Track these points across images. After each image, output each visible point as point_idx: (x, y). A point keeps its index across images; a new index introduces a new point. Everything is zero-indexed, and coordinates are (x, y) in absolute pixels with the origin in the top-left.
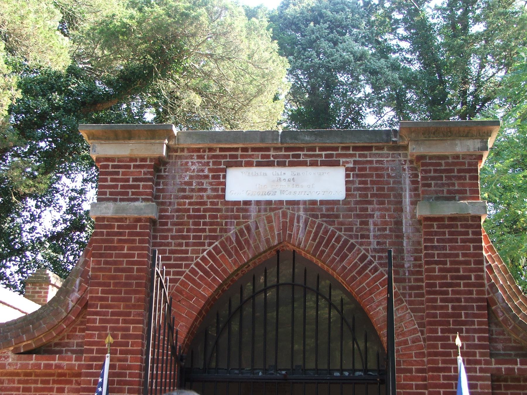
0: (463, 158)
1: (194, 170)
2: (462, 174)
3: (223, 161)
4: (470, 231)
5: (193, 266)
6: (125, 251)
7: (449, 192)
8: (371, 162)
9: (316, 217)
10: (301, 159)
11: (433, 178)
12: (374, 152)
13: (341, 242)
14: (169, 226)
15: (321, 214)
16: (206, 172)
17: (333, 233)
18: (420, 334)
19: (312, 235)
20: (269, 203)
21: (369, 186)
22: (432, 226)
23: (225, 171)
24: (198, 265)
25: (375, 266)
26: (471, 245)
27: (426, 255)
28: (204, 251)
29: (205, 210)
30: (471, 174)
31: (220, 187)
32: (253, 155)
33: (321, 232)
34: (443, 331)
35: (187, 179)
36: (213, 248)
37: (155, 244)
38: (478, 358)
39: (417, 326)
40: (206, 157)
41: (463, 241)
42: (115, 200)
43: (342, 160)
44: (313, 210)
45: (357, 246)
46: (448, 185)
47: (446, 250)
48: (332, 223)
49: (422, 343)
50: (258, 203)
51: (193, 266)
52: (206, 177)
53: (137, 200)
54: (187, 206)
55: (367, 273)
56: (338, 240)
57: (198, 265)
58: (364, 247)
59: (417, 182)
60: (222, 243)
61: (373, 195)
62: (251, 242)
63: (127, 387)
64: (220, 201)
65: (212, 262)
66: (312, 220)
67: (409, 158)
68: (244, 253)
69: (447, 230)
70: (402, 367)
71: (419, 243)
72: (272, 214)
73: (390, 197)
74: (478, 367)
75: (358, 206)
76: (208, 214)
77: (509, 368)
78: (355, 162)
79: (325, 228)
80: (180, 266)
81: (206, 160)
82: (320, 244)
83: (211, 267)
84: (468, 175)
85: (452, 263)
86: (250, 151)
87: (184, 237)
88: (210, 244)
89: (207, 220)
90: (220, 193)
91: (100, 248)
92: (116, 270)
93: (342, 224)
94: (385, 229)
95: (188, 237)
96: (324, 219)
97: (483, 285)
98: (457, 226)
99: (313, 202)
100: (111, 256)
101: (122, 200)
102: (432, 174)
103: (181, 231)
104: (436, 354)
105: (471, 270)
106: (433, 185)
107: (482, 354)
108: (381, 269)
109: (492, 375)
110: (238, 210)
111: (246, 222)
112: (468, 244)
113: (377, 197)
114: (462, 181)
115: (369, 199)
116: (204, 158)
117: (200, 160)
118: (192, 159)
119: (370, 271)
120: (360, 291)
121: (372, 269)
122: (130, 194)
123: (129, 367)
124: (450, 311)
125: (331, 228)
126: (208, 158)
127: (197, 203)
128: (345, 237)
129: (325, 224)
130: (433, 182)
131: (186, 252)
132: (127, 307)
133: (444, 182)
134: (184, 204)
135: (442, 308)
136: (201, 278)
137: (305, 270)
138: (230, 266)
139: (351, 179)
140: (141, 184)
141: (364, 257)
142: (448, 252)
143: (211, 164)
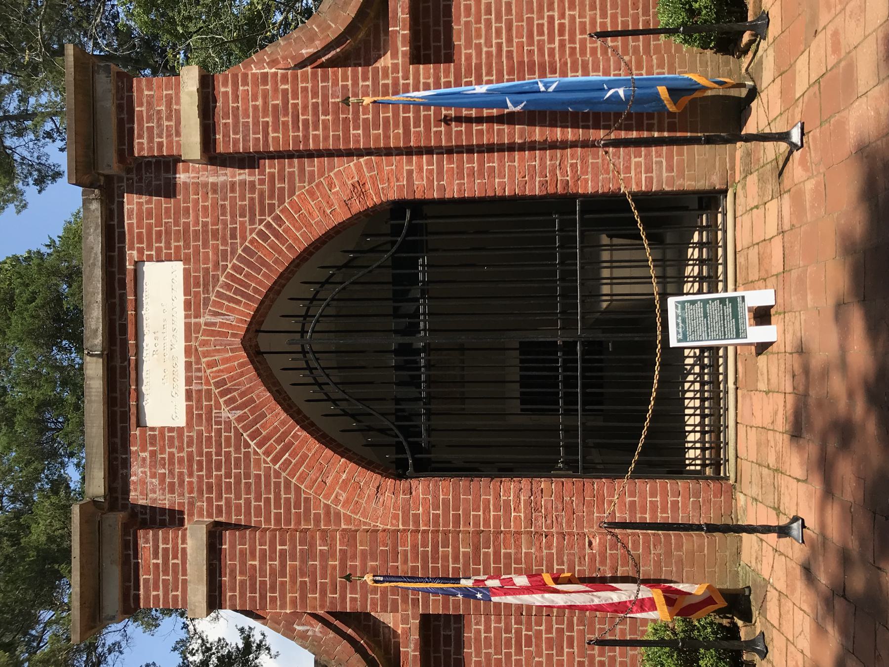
0: (122, 98)
1: (142, 472)
2: (145, 100)
5: (277, 467)
6: (257, 563)
7: (169, 118)
9: (207, 301)
16: (146, 454)
17: (230, 277)
19: (231, 305)
20: (188, 366)
21: (163, 228)
24: (275, 461)
25: (273, 219)
26: (241, 88)
28: (256, 453)
31: (167, 434)
32: (120, 390)
33: (228, 293)
35: (156, 481)
38: (390, 81)
41: (236, 98)
42: (185, 582)
46: (159, 119)
48: (216, 279)
50: (189, 381)
52: (153, 454)
53: (184, 550)
54: (195, 480)
56: (238, 270)
58: (248, 233)
61: (177, 224)
62: (243, 389)
63: (441, 549)
64: (186, 434)
65: (272, 441)
67: (124, 174)
70: (405, 183)
74: (401, 82)
75: (192, 244)
76: (205, 450)
79: (222, 287)
80: (277, 485)
82: (244, 294)
83: (278, 441)
85: (265, 115)
86: (114, 395)
87: (238, 482)
88: (247, 445)
89: (214, 450)
93: (216, 265)
94: (223, 207)
99: (187, 305)
100: (263, 583)
101: (185, 573)
105: (276, 89)
106: (160, 140)
109: (412, 63)
111: (216, 396)
112: (240, 93)
113: (179, 217)
115: (181, 228)
119: (280, 226)
121: (277, 225)
122: (175, 561)
123: (415, 547)
125: (222, 279)
127: (190, 466)
128: (234, 261)
129: (217, 289)
130: (156, 140)
133: (154, 125)
135: (326, 128)
136: (293, 455)
137: (283, 316)
139: (153, 253)
140: (161, 546)
141: (261, 234)
142: (250, 120)
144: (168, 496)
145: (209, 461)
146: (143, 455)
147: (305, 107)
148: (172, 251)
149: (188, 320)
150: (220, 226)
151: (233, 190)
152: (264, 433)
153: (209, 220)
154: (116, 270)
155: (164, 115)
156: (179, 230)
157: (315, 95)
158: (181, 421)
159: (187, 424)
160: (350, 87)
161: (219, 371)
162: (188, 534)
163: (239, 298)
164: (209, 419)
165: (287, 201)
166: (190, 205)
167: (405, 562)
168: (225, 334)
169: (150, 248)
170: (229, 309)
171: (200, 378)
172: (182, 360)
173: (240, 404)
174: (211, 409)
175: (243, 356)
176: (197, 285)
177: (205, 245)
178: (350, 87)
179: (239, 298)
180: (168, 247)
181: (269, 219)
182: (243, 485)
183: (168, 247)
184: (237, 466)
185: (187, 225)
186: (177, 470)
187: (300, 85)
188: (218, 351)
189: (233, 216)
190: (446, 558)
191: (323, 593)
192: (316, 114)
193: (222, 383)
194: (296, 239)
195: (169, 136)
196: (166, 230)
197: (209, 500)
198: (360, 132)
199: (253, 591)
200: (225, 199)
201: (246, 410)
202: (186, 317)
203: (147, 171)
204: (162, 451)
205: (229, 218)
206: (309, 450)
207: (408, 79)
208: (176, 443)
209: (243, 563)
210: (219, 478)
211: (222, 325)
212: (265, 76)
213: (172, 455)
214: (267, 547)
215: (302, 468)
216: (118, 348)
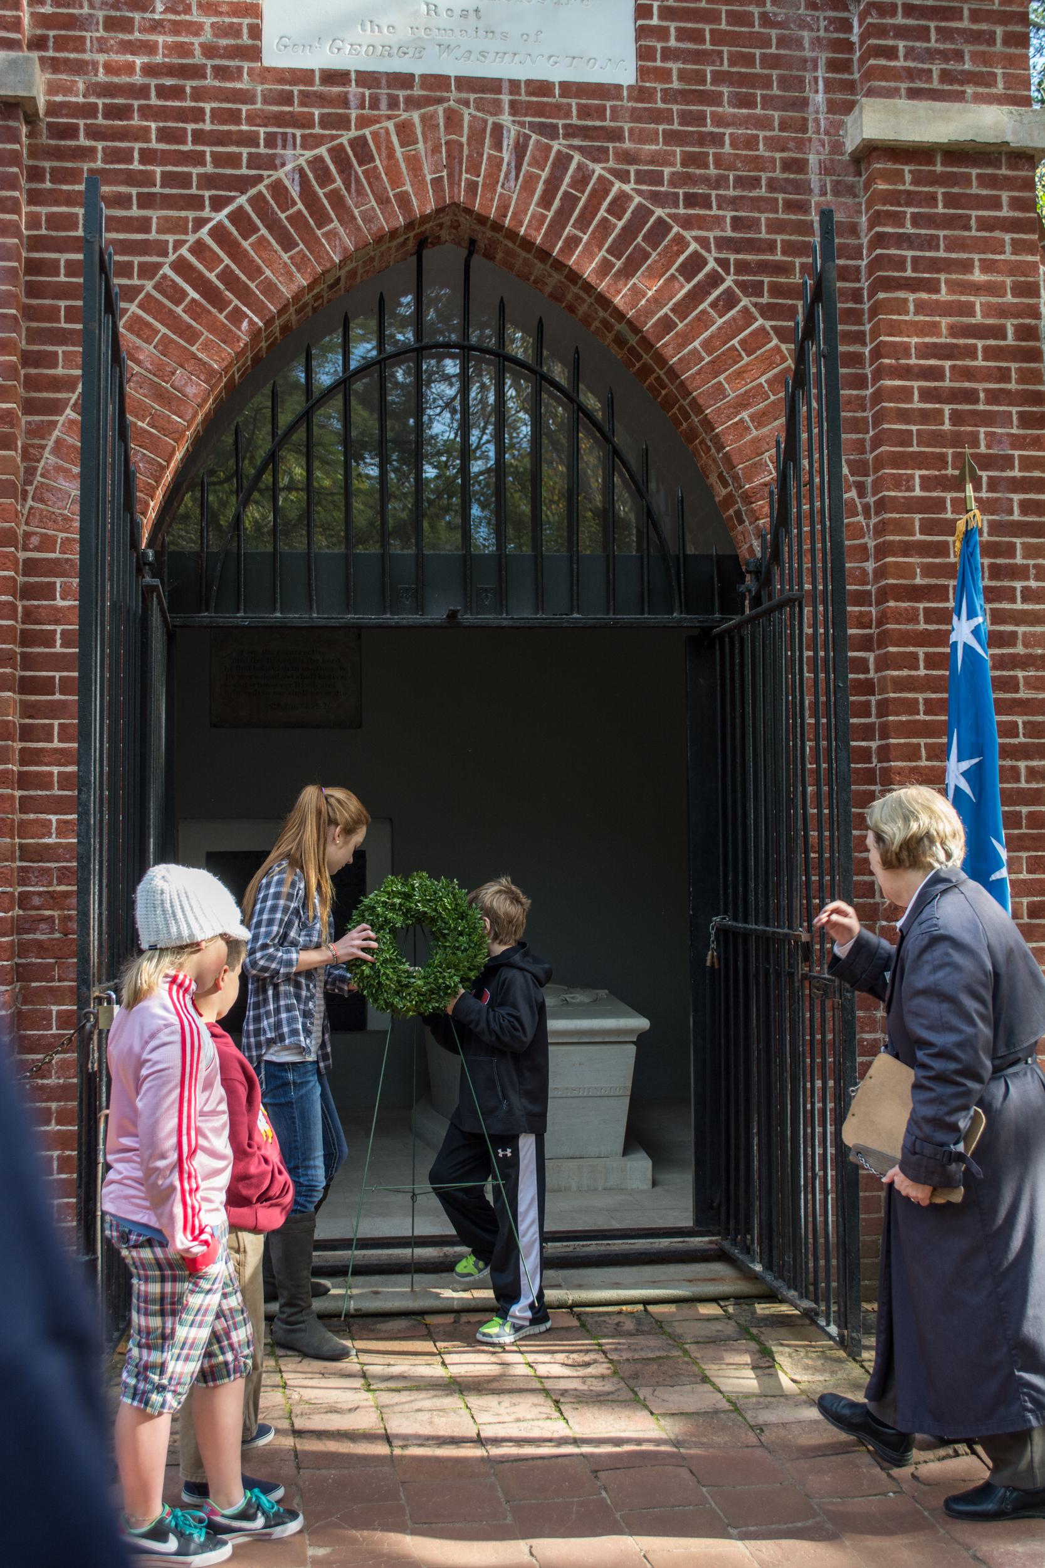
2: (984, 26)
4: (1005, 196)
5: (166, 270)
9: (550, 131)
11: (901, 32)
13: (628, 215)
14: (83, 141)
15: (565, 126)
17: (604, 187)
19: (540, 187)
20: (404, 80)
21: (708, 46)
22: (898, 176)
24: (181, 266)
25: (729, 290)
26: (1007, 237)
27: (876, 264)
28: (200, 223)
30: (1010, 28)
31: (246, 21)
33: (567, 180)
34: (926, 483)
37: (34, 198)
38: (1019, 560)
41: (985, 225)
45: (676, 229)
46: (945, 56)
47: (937, 249)
48: (598, 155)
49: (860, 518)
50: (367, 79)
54: (138, 79)
57: (181, 266)
59: (849, 46)
60: (258, 202)
61: (718, 77)
64: (246, 65)
65: (227, 261)
66: (538, 141)
69: (940, 191)
72: (416, 116)
73: (769, 86)
74: (1018, 585)
75: (675, 107)
76: (208, 107)
79: (580, 167)
83: (227, 277)
84: (999, 31)
87: (131, 178)
88: (218, 204)
89: (208, 126)
90: (245, 40)
93: (628, 157)
94: (755, 183)
95: (146, 179)
96: (577, 142)
98: (966, 180)
99: (542, 88)
102: (900, 20)
103: (125, 156)
104: (907, 549)
105: (1003, 312)
106: (901, 53)
108: (745, 301)
110: (307, 98)
112: (997, 234)
113: (731, 84)
115: (709, 87)
119: (713, 305)
120: (687, 362)
121: (718, 299)
124: (947, 426)
125: (598, 169)
128: (637, 199)
129: (577, 158)
130: (901, 44)
131: (143, 225)
133: (933, 44)
134: (130, 68)
135: (925, 416)
136: (194, 309)
139: (655, 21)
141: (694, 264)
142: (942, 254)
144: (100, 14)
145: (183, 115)
147: (968, 374)
148: (659, 63)
149: (506, 87)
150: (712, 171)
151: (790, 206)
152: (246, 244)
153: (727, 149)
155: (951, 66)
156: (703, 82)
157: (994, 397)
159: (268, 70)
160: (1009, 474)
162: (13, 54)
163: (557, 203)
164: (280, 120)
165: (768, 324)
166: (758, 111)
168: (474, 169)
170: (532, 179)
171: (375, 105)
172: (418, 69)
173: (315, 193)
174: (303, 126)
175: (424, 204)
176: (584, 112)
177: (672, 137)
178: (1009, 474)
179: (557, 203)
180: (667, 54)
181: (729, 282)
182: (123, 189)
183: (667, 54)
185: (714, 99)
186: (161, 39)
187: (1014, 366)
188: (436, 150)
189: (735, 203)
192: (954, 396)
193: (365, 157)
194: (685, 338)
195: (911, 74)
197: (89, 111)
198: (918, 492)
200: (772, 185)
201: (300, 206)
202: (514, 85)
203: (831, 21)
205: (731, 193)
206: (206, 347)
207: (1025, 600)
208: (224, 42)
211: (496, 163)
215: (164, 330)
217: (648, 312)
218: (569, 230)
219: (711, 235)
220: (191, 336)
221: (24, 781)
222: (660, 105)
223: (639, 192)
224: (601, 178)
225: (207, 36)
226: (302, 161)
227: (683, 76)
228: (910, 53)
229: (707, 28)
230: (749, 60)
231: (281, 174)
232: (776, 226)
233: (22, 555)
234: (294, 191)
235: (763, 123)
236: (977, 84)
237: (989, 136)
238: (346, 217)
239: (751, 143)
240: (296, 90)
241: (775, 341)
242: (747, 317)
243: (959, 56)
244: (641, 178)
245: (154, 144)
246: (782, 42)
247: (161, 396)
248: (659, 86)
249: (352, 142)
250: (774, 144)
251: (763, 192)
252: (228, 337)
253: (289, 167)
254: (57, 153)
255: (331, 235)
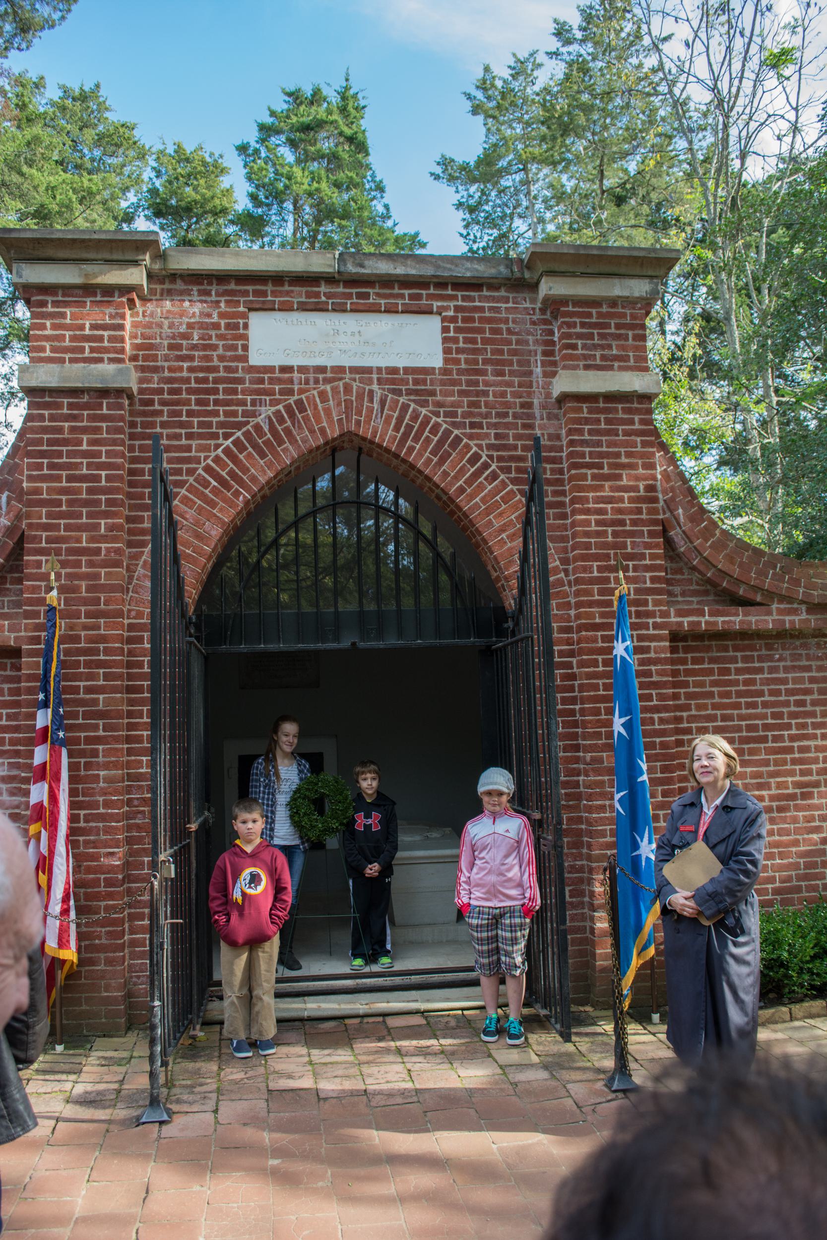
1: (194, 313)
2: (622, 332)
3: (242, 299)
5: (200, 471)
6: (85, 447)
8: (481, 309)
9: (399, 393)
10: (371, 301)
11: (580, 336)
12: (485, 293)
14: (157, 407)
16: (215, 318)
17: (427, 420)
18: (562, 575)
19: (394, 421)
20: (322, 369)
21: (480, 346)
22: (580, 410)
23: (244, 316)
24: (208, 469)
25: (494, 471)
26: (639, 439)
27: (571, 455)
28: (217, 446)
29: (216, 381)
31: (240, 343)
33: (408, 417)
35: (183, 329)
36: (233, 443)
37: (132, 437)
38: (650, 608)
39: (558, 563)
40: (213, 293)
41: (627, 433)
42: (62, 361)
43: (436, 304)
44: (393, 382)
45: (465, 440)
46: (602, 347)
48: (424, 404)
49: (567, 588)
50: (302, 369)
51: (200, 471)
52: (216, 326)
53: (100, 360)
54: (185, 374)
55: (481, 483)
57: (208, 469)
59: (553, 343)
60: (247, 434)
61: (486, 362)
63: (101, 671)
64: (240, 365)
65: (232, 465)
68: (284, 450)
69: (602, 417)
71: (558, 437)
72: (328, 388)
74: (651, 621)
76: (221, 387)
77: (693, 622)
78: (457, 309)
79: (414, 410)
81: (214, 298)
82: (406, 436)
83: (232, 474)
84: (630, 333)
86: (286, 284)
87: (182, 425)
88: (226, 436)
89: (221, 397)
90: (240, 352)
91: (40, 442)
92: (70, 479)
93: (439, 404)
94: (506, 415)
95: (189, 425)
96: (412, 397)
97: (655, 500)
99: (394, 370)
100: (60, 455)
101: (72, 361)
102: (578, 330)
103: (179, 414)
104: (591, 604)
107: (656, 603)
108: (502, 477)
111: (286, 400)
112: (633, 438)
113: (492, 365)
114: (622, 342)
115: (481, 367)
116: (211, 295)
117: (203, 298)
118: (190, 295)
119: (486, 479)
122: (87, 350)
123: (104, 639)
124: (610, 539)
125: (424, 411)
126: (217, 295)
128: (445, 426)
129: (413, 405)
130: (580, 342)
131: (188, 449)
132: (91, 540)
133: (596, 341)
135: (598, 534)
136: (215, 491)
138: (262, 472)
139: (452, 334)
140: (106, 334)
142: (604, 449)
143: (222, 305)
144: (166, 343)
145: (208, 391)
146: (215, 315)
147: (620, 511)
149: (375, 370)
150: (483, 410)
151: (525, 426)
152: (241, 456)
153: (491, 398)
154: (432, 291)
155: (606, 352)
156: (478, 364)
157: (634, 523)
158: (255, 359)
159: (252, 367)
160: (644, 562)
161: (316, 406)
162: (120, 366)
164: (259, 392)
165: (515, 488)
166: (507, 378)
167: (86, 627)
169: (458, 330)
170: (389, 417)
172: (329, 363)
174: (270, 395)
175: (333, 432)
176: (416, 382)
177: (462, 393)
178: (644, 562)
180: (459, 351)
181: (494, 467)
182: (178, 431)
183: (459, 351)
184: (201, 425)
185: (483, 373)
186: (196, 353)
187: (644, 506)
188: (339, 404)
189: (495, 426)
190: (91, 677)
191: (46, 527)
192: (614, 523)
193: (302, 409)
194: (472, 497)
195: (585, 357)
196: (478, 349)
197: (160, 391)
198: (596, 574)
199: (50, 442)
200: (515, 416)
201: (269, 435)
202: (379, 370)
204: (220, 337)
205: (494, 420)
206: (221, 510)
207: (654, 628)
208: (229, 353)
209: (84, 430)
210: (187, 402)
212: (652, 466)
213: (214, 347)
214: (103, 459)
215: (199, 502)
216: (341, 289)
217: (452, 484)
218: (409, 443)
219: (484, 443)
220: (213, 505)
221: (129, 739)
222: (455, 377)
223: (445, 422)
224: (425, 415)
225: (220, 351)
226: (270, 413)
227: (467, 361)
228: (584, 347)
229: (479, 336)
230: (501, 352)
231: (259, 419)
232: (517, 437)
233: (126, 622)
234: (266, 428)
235: (509, 384)
236: (620, 361)
237: (628, 388)
238: (293, 440)
239: (503, 394)
240: (266, 376)
241: (519, 497)
242: (504, 485)
243: (610, 347)
244: (446, 415)
245: (194, 407)
246: (518, 342)
247: (198, 536)
248: (455, 367)
249: (295, 402)
250: (515, 395)
251: (510, 419)
252: (232, 505)
253: (263, 416)
254: (144, 414)
255: (285, 450)
